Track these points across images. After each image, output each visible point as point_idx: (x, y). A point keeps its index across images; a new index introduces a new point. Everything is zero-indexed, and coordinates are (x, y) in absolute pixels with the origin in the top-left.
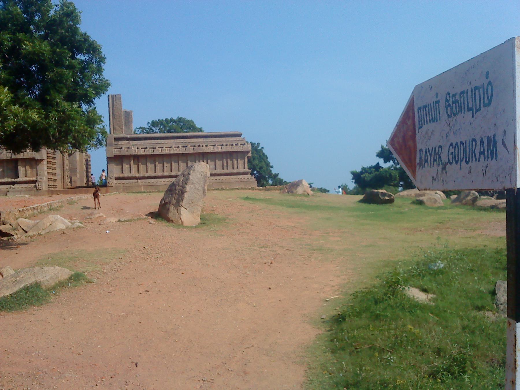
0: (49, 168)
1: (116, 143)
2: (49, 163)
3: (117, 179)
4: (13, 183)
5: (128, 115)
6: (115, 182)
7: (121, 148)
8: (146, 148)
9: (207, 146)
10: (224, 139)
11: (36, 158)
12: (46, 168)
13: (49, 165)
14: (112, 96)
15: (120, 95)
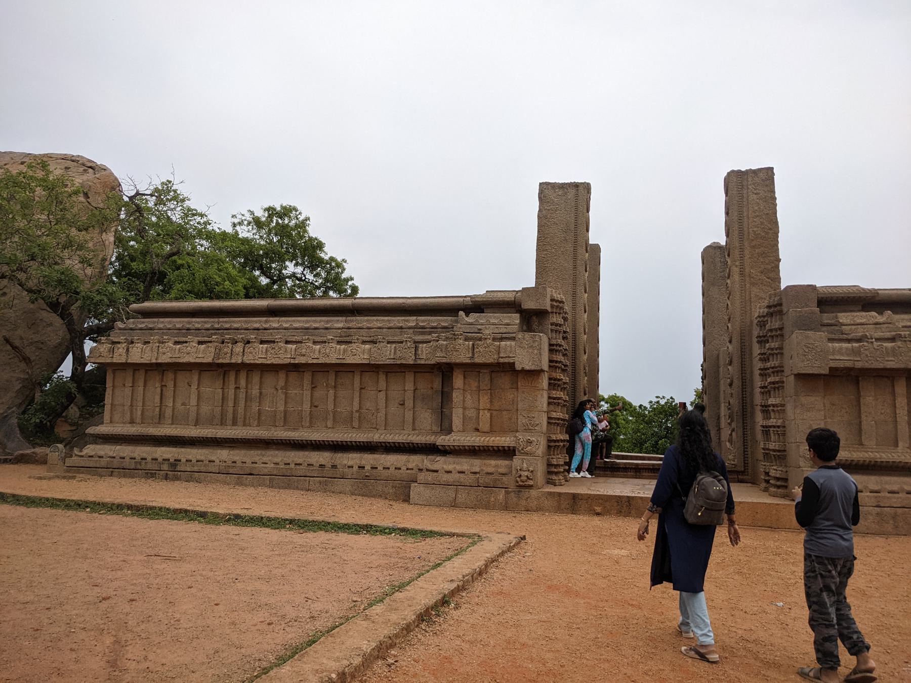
1: (827, 318)
2: (554, 384)
4: (431, 450)
11: (518, 367)
12: (543, 401)
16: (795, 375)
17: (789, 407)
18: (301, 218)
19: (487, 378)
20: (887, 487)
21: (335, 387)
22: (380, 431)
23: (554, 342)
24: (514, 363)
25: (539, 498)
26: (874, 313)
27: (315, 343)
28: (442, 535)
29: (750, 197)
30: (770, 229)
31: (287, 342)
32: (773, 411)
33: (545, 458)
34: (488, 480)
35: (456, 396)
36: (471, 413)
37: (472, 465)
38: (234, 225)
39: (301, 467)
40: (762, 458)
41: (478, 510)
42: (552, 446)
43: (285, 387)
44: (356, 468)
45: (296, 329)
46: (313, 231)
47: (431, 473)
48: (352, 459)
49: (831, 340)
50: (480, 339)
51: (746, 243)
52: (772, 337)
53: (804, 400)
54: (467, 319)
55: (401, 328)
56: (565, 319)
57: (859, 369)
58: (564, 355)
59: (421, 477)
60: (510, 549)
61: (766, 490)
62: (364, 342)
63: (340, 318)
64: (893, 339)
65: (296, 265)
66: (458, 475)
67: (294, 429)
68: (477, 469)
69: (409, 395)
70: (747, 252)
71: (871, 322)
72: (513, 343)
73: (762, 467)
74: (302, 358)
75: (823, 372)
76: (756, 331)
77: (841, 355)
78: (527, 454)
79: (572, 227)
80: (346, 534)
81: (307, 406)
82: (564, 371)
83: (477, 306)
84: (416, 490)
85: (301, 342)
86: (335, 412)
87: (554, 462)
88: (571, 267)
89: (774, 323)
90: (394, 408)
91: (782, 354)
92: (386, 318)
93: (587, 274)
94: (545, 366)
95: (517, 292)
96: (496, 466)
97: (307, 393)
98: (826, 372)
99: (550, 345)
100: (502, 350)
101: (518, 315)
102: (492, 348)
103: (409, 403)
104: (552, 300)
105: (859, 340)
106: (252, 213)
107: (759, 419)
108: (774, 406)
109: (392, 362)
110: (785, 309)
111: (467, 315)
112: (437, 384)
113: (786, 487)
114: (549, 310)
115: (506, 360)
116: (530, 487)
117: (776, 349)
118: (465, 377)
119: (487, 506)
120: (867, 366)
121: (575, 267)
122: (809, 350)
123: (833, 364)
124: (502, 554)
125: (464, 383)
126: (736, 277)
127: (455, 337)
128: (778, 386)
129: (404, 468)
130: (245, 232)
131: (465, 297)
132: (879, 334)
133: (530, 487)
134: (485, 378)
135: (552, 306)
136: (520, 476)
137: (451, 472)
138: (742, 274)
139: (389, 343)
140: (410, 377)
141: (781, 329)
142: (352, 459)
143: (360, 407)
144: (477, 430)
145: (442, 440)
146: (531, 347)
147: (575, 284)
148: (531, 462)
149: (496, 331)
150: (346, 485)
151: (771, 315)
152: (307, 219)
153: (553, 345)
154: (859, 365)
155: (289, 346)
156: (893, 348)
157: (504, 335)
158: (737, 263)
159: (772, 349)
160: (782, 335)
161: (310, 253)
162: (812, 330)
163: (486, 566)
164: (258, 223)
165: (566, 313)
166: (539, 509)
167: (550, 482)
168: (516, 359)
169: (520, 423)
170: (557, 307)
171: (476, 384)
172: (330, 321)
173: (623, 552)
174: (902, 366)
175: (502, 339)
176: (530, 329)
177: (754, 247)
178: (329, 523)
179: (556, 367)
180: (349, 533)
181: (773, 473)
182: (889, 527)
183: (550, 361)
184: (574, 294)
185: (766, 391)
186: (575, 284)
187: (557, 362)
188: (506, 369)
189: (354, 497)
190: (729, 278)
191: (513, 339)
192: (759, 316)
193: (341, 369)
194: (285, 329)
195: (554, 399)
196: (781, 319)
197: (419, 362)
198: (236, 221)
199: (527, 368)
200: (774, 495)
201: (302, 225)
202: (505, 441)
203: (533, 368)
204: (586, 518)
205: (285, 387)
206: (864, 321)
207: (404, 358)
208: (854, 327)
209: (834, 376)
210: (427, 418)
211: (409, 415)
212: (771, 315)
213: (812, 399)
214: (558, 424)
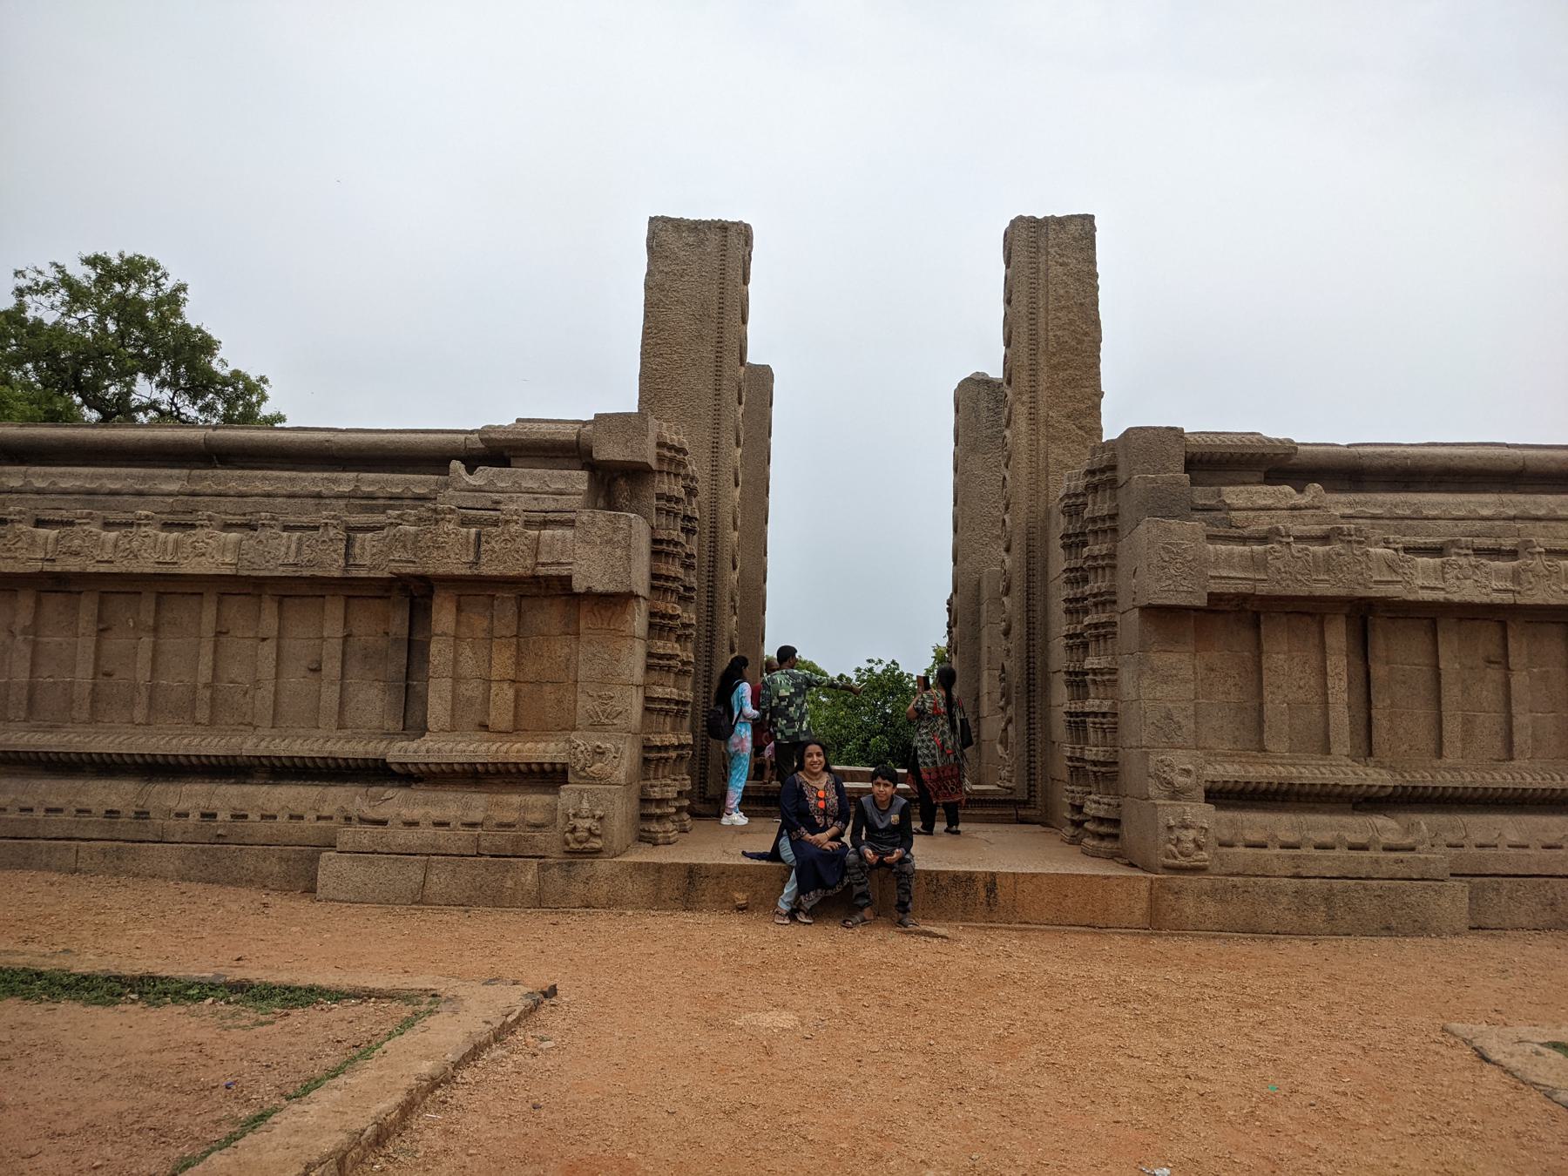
0: (656, 664)
1: (1202, 495)
2: (659, 625)
3: (1220, 796)
4: (375, 772)
6: (1201, 813)
8: (1437, 551)
11: (579, 585)
12: (634, 661)
13: (662, 647)
16: (1142, 609)
17: (1126, 676)
18: (168, 285)
19: (510, 610)
20: (1311, 835)
21: (156, 630)
22: (260, 732)
23: (663, 535)
24: (569, 578)
25: (613, 877)
26: (1287, 488)
27: (107, 525)
28: (338, 996)
29: (1051, 268)
30: (1086, 334)
31: (39, 523)
32: (1094, 682)
33: (636, 786)
34: (501, 839)
35: (439, 652)
36: (471, 690)
37: (467, 807)
38: (20, 292)
39: (61, 816)
40: (1066, 776)
41: (475, 911)
42: (651, 759)
43: (35, 629)
44: (194, 817)
45: (65, 492)
46: (193, 314)
47: (369, 828)
48: (192, 796)
49: (1212, 538)
50: (495, 524)
51: (1042, 360)
52: (1095, 533)
53: (1159, 659)
54: (468, 478)
55: (319, 496)
56: (691, 492)
57: (1263, 598)
58: (687, 567)
59: (346, 836)
60: (500, 1035)
61: (1074, 841)
62: (227, 527)
63: (176, 472)
64: (1325, 539)
65: (162, 384)
66: (433, 830)
67: (53, 728)
68: (477, 816)
69: (333, 647)
70: (1043, 377)
71: (1283, 504)
72: (569, 533)
73: (1065, 794)
74: (72, 560)
75: (1197, 603)
76: (1060, 525)
77: (1232, 569)
78: (592, 779)
79: (714, 312)
80: (77, 1006)
81: (84, 675)
82: (684, 600)
83: (495, 451)
84: (330, 866)
85: (71, 524)
86: (153, 689)
87: (656, 793)
88: (710, 392)
89: (1099, 506)
90: (295, 679)
91: (1114, 567)
92: (286, 474)
93: (741, 409)
94: (641, 584)
95: (585, 423)
96: (523, 808)
97: (87, 644)
98: (1202, 602)
99: (655, 541)
100: (543, 549)
101: (584, 474)
102: (520, 543)
103: (332, 668)
104: (661, 445)
105: (1263, 540)
106: (60, 269)
107: (1061, 697)
108: (1095, 672)
109: (289, 572)
110: (1122, 476)
111: (470, 470)
112: (399, 623)
113: (1115, 837)
114: (654, 464)
115: (553, 571)
116: (596, 853)
117: (1103, 557)
118: (459, 609)
119: (497, 900)
120: (1278, 590)
121: (718, 393)
122: (1171, 557)
123: (1215, 587)
124: (476, 1052)
125: (458, 622)
126: (1022, 424)
127: (437, 517)
128: (1104, 633)
129: (312, 816)
130: (45, 310)
131: (472, 432)
132: (1297, 528)
133: (596, 853)
134: (506, 611)
135: (660, 459)
136: (574, 830)
137: (415, 824)
138: (1032, 418)
139: (286, 528)
140: (334, 610)
141: (1113, 517)
142: (190, 796)
143: (215, 676)
144: (484, 727)
145: (399, 751)
146: (609, 541)
147: (716, 428)
148: (603, 800)
149: (534, 506)
150: (168, 857)
151: (1093, 488)
152: (183, 288)
153: (660, 542)
154: (1263, 589)
155: (42, 531)
156: (1328, 556)
157: (551, 516)
158: (1025, 398)
159: (1095, 558)
160: (1114, 530)
161: (188, 358)
162: (1174, 517)
163: (408, 1109)
164: (77, 295)
165: (693, 479)
166: (614, 903)
167: (647, 838)
168: (575, 568)
169: (580, 711)
170: (671, 460)
171: (486, 624)
172: (153, 478)
173: (786, 1019)
174: (1343, 592)
175: (545, 524)
176: (611, 505)
177: (1054, 367)
178: (39, 975)
179: (666, 590)
180: (88, 1003)
181: (1091, 809)
182: (1318, 918)
183: (654, 576)
184: (715, 447)
185: (1079, 644)
186: (716, 428)
187: (667, 578)
188: (550, 590)
189: (184, 886)
190: (1007, 426)
191: (570, 524)
192: (1067, 496)
193: (168, 588)
194: (39, 492)
195: (661, 657)
196: (1114, 498)
197: (354, 573)
198: (23, 283)
199: (599, 588)
200: (1095, 854)
201: (174, 300)
202: (546, 750)
203: (611, 588)
204: (714, 918)
205: (35, 629)
206: (1269, 502)
207: (321, 565)
208: (1252, 514)
209: (1213, 611)
210: (372, 701)
211: (330, 695)
212: (1093, 488)
213: (1173, 658)
214: (667, 712)
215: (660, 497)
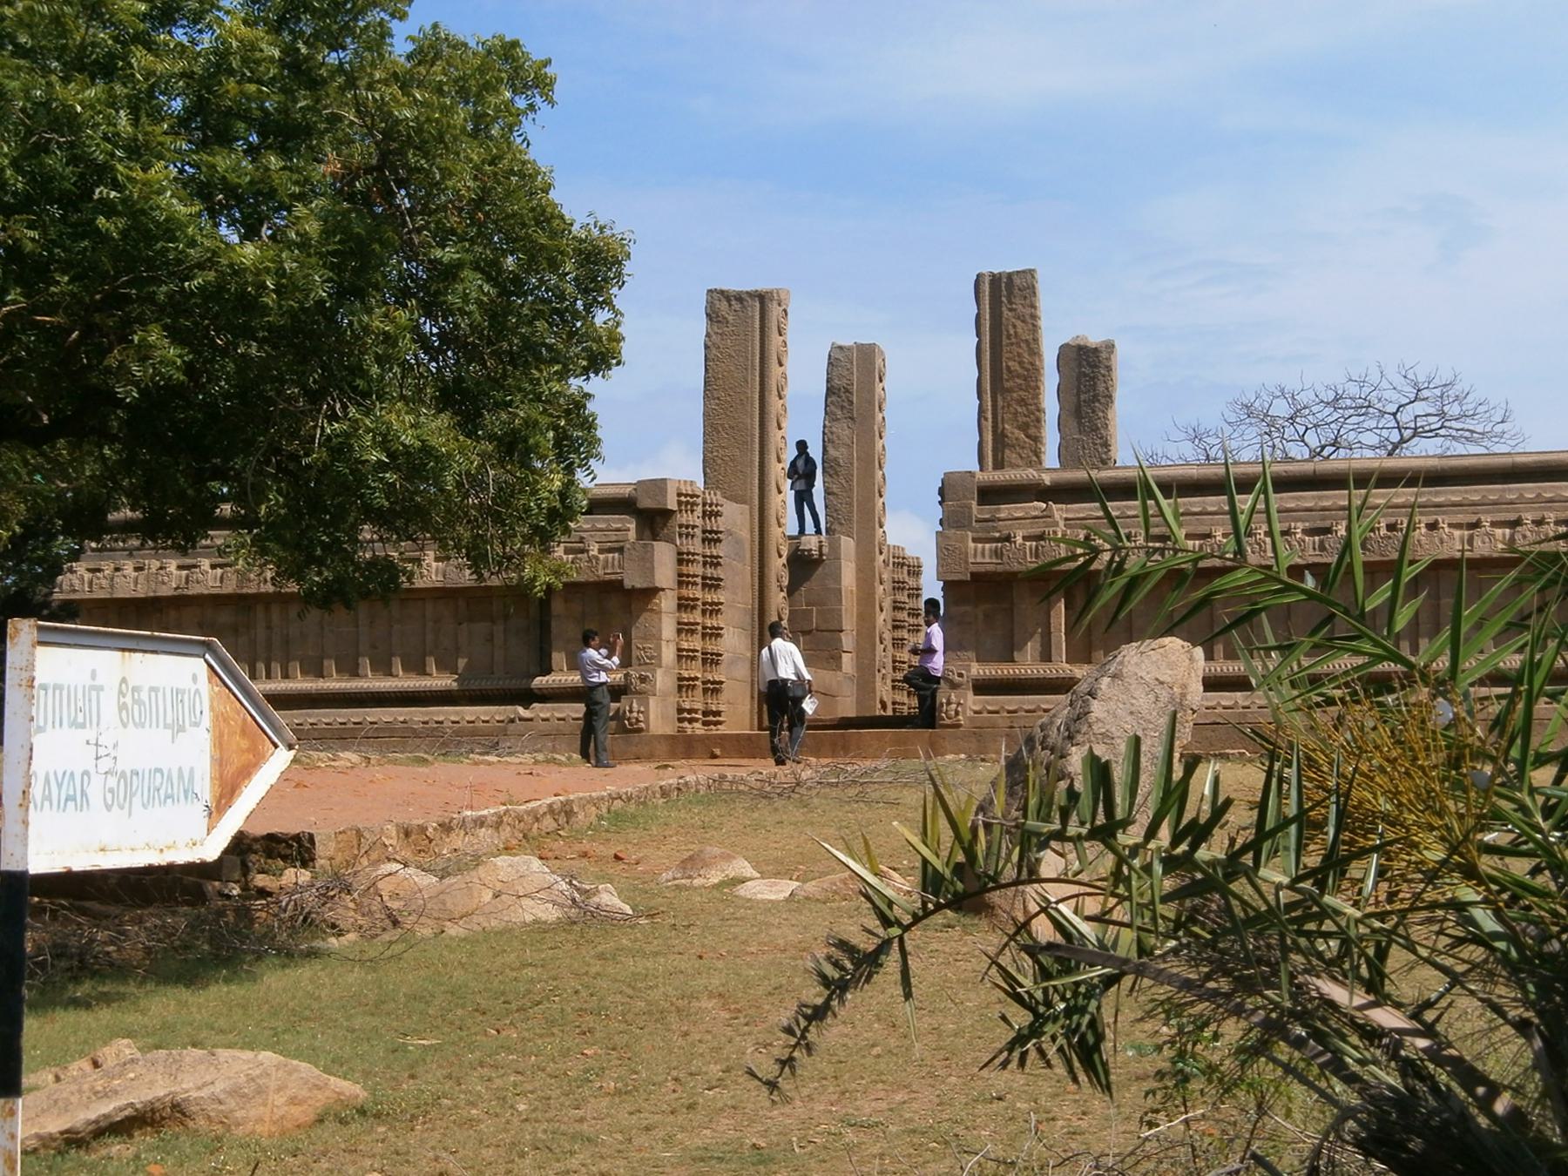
0: (684, 629)
1: (986, 512)
2: (684, 605)
5: (1088, 370)
7: (1008, 539)
9: (1433, 526)
10: (1530, 489)
11: (628, 584)
12: (668, 628)
13: (685, 617)
14: (995, 280)
15: (1031, 272)
24: (621, 581)
104: (679, 495)
115: (613, 577)
123: (973, 568)
135: (680, 503)
215: (681, 526)
